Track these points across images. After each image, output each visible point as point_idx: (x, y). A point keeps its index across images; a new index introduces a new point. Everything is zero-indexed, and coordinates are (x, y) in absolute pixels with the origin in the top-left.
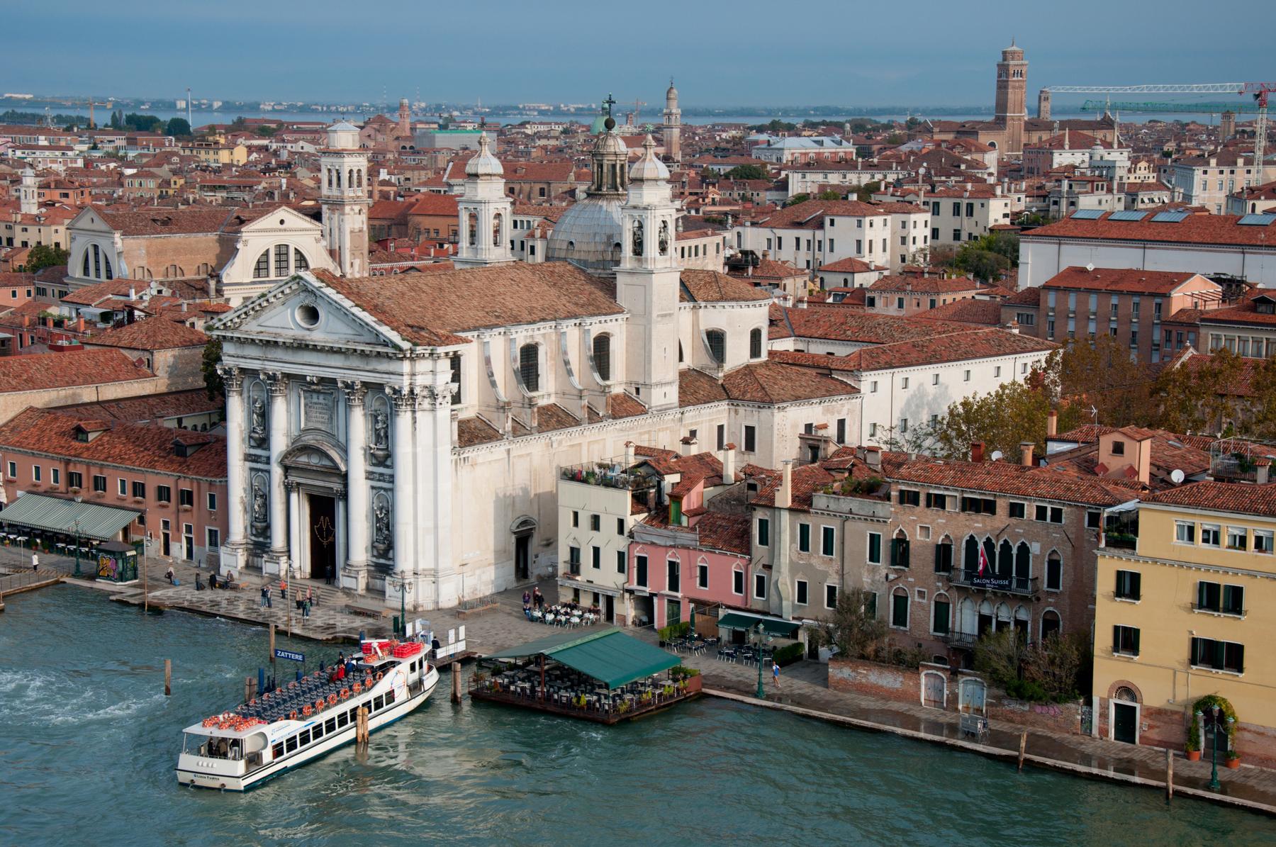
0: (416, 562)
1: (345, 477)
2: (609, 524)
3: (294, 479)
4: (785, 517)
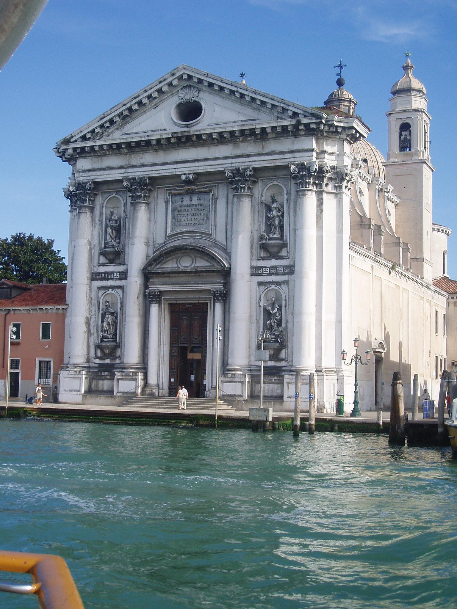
0: (319, 359)
1: (226, 274)
3: (155, 287)
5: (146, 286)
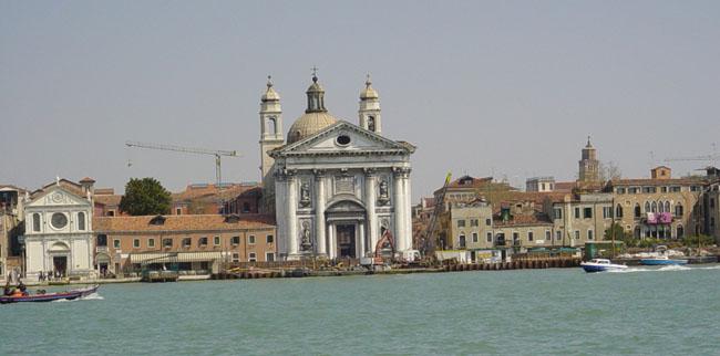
1: (366, 213)
2: (482, 222)
4: (569, 206)
5: (326, 218)
